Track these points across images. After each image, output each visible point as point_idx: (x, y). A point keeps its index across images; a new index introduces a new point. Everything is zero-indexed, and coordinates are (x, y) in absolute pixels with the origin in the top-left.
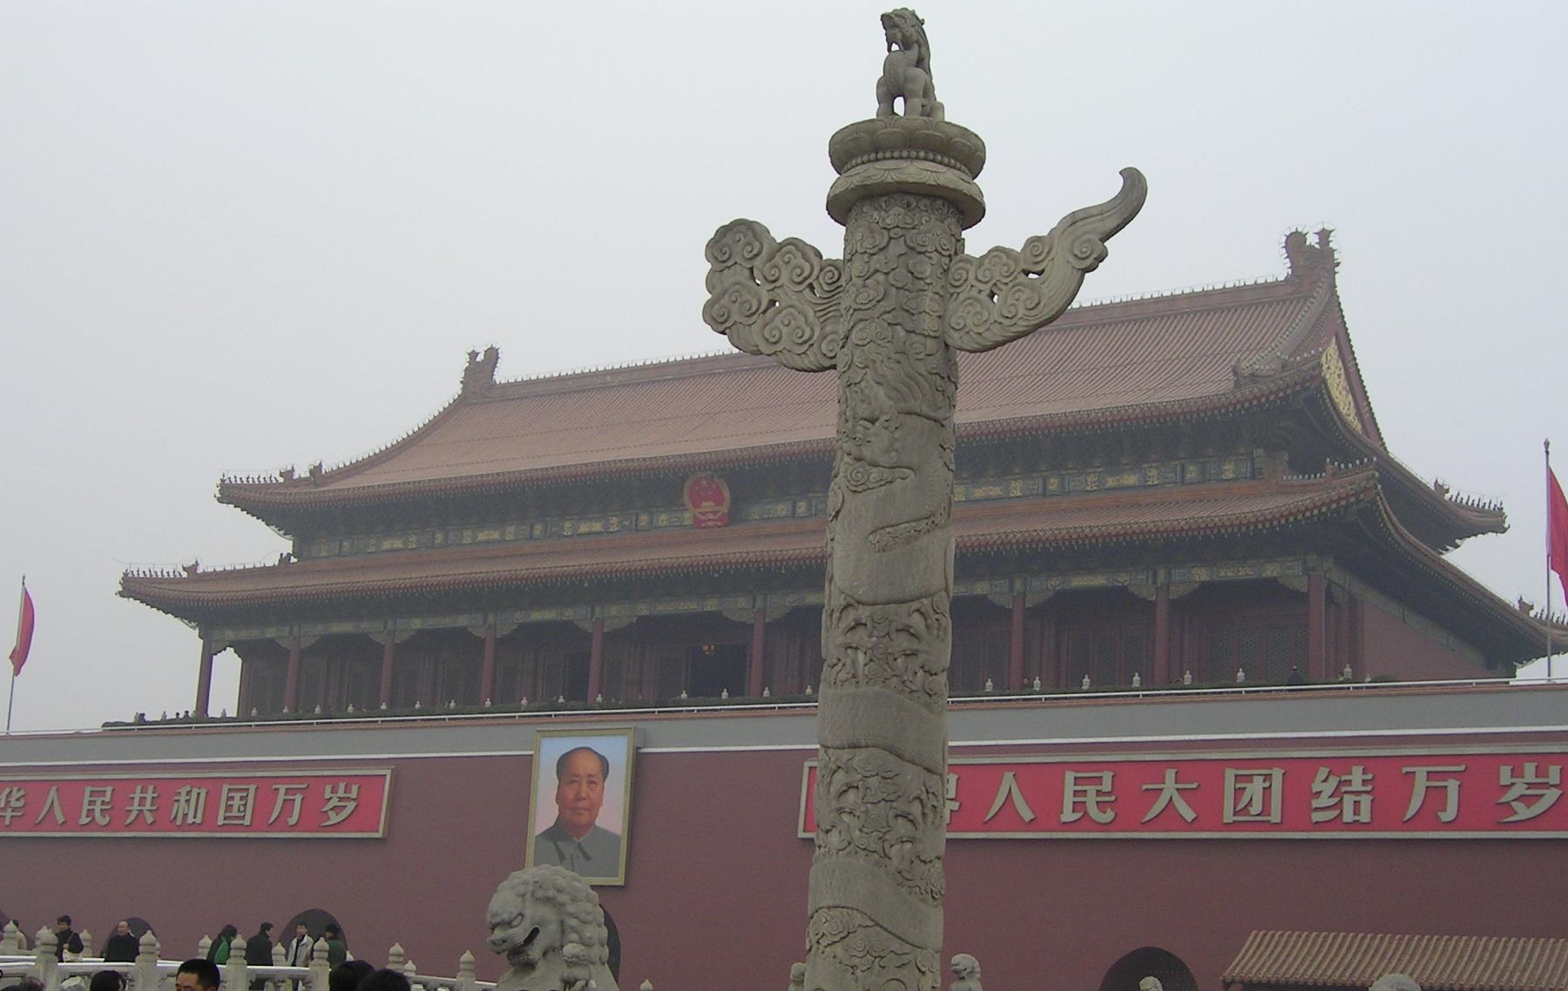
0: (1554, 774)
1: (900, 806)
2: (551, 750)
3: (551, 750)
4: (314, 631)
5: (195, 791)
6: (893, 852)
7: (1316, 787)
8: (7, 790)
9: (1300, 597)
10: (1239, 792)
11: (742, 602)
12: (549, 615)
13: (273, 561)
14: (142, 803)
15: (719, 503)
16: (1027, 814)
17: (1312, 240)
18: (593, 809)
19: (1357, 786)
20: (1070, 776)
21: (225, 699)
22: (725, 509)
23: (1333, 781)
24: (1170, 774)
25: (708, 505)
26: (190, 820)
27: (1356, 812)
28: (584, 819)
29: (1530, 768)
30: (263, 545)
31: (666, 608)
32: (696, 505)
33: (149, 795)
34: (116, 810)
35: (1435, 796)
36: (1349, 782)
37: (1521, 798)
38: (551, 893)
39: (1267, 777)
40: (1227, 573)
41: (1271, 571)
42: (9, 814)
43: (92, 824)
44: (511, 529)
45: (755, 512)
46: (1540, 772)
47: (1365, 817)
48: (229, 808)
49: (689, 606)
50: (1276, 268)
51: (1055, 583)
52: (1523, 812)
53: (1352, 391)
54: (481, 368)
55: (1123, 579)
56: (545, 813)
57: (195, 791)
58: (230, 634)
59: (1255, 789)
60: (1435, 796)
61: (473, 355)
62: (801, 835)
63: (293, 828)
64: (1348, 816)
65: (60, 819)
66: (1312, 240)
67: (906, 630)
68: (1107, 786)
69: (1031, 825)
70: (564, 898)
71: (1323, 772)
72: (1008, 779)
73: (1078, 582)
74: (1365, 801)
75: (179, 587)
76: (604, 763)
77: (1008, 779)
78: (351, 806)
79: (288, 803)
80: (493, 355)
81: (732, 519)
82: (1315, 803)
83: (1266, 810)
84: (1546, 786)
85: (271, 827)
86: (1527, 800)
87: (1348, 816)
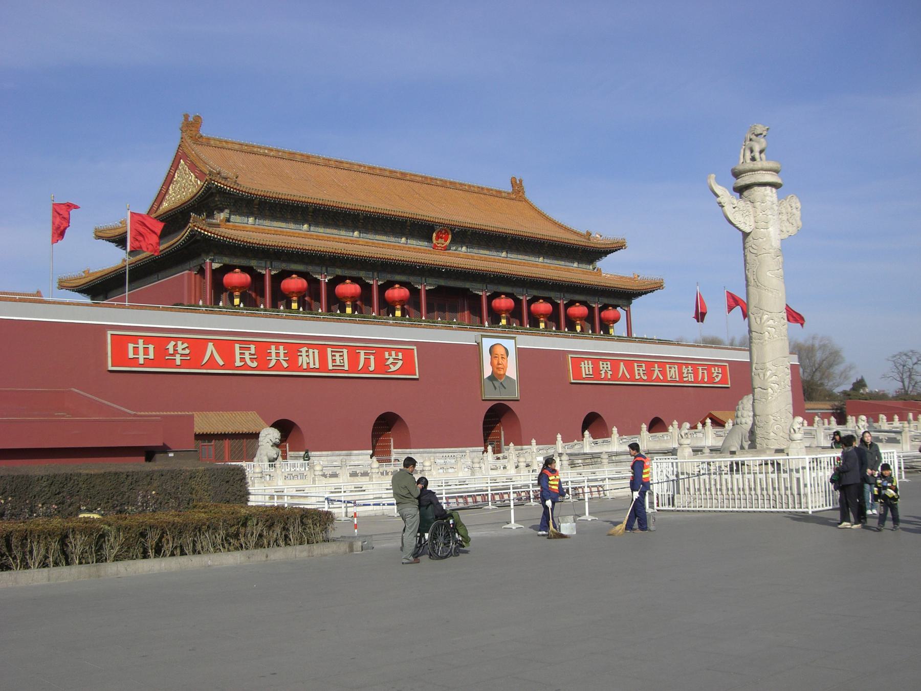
2: (487, 343)
8: (173, 343)
18: (505, 368)
26: (312, 366)
28: (502, 372)
43: (245, 366)
56: (488, 371)
57: (311, 351)
59: (673, 370)
63: (372, 372)
69: (222, 367)
76: (506, 349)
78: (400, 363)
79: (367, 360)
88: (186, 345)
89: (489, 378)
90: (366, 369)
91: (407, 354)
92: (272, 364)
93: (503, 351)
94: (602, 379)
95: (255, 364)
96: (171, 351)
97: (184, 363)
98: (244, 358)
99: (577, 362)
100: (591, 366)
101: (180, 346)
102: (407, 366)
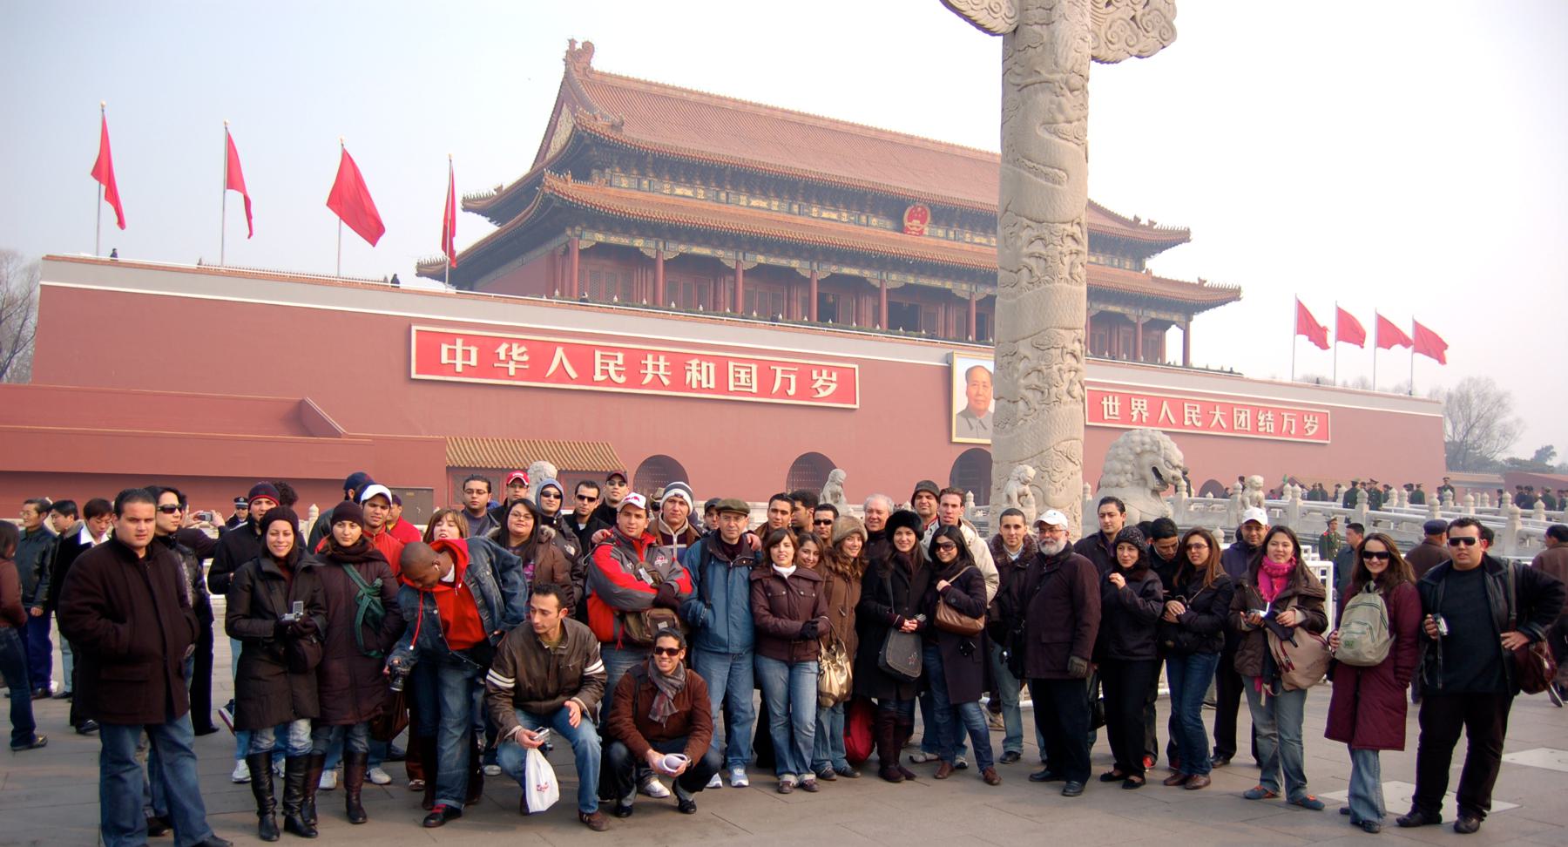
5: (704, 365)
11: (965, 287)
12: (705, 251)
31: (924, 281)
43: (610, 382)
48: (738, 379)
49: (937, 283)
78: (833, 387)
79: (786, 383)
88: (523, 349)
89: (963, 414)
90: (783, 392)
91: (846, 378)
92: (646, 381)
95: (622, 380)
96: (503, 357)
101: (516, 351)
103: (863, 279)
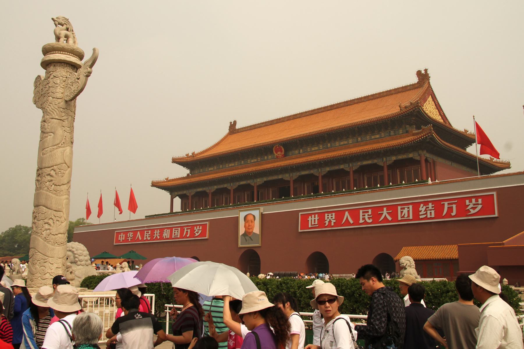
0: (480, 201)
1: (46, 221)
2: (242, 215)
3: (242, 215)
4: (193, 192)
6: (44, 233)
7: (420, 209)
9: (418, 162)
10: (402, 212)
11: (287, 175)
13: (185, 175)
14: (157, 234)
15: (281, 152)
16: (351, 222)
17: (423, 72)
18: (252, 228)
19: (430, 208)
20: (361, 211)
21: (177, 208)
22: (283, 153)
23: (425, 207)
24: (385, 209)
25: (279, 153)
27: (431, 214)
28: (251, 231)
29: (474, 200)
30: (183, 172)
32: (277, 153)
33: (158, 232)
34: (152, 236)
35: (450, 209)
36: (428, 207)
37: (472, 208)
38: (71, 249)
39: (408, 208)
40: (400, 157)
41: (411, 155)
42: (130, 238)
43: (147, 240)
44: (236, 163)
45: (290, 153)
46: (477, 201)
47: (433, 216)
48: (175, 234)
50: (415, 80)
51: (359, 164)
52: (473, 212)
53: (437, 109)
54: (233, 125)
55: (375, 161)
56: (242, 230)
58: (176, 193)
59: (405, 211)
60: (450, 209)
61: (231, 123)
62: (300, 231)
63: (188, 238)
64: (429, 216)
65: (140, 239)
66: (423, 72)
67: (49, 175)
68: (370, 213)
70: (74, 250)
71: (422, 205)
72: (347, 213)
73: (365, 163)
74: (433, 212)
75: (169, 183)
76: (254, 216)
77: (347, 213)
78: (200, 231)
79: (187, 232)
80: (235, 122)
81: (285, 155)
82: (420, 213)
83: (409, 216)
84: (478, 204)
85: (183, 238)
86: (474, 208)
87: (429, 216)
93: (252, 218)
94: (326, 227)
97: (132, 240)
98: (365, 218)
99: (305, 218)
100: (317, 218)
101: (131, 234)
102: (203, 234)
103: (312, 174)
